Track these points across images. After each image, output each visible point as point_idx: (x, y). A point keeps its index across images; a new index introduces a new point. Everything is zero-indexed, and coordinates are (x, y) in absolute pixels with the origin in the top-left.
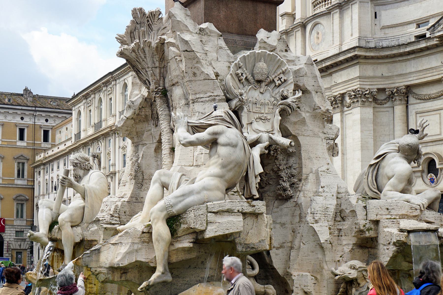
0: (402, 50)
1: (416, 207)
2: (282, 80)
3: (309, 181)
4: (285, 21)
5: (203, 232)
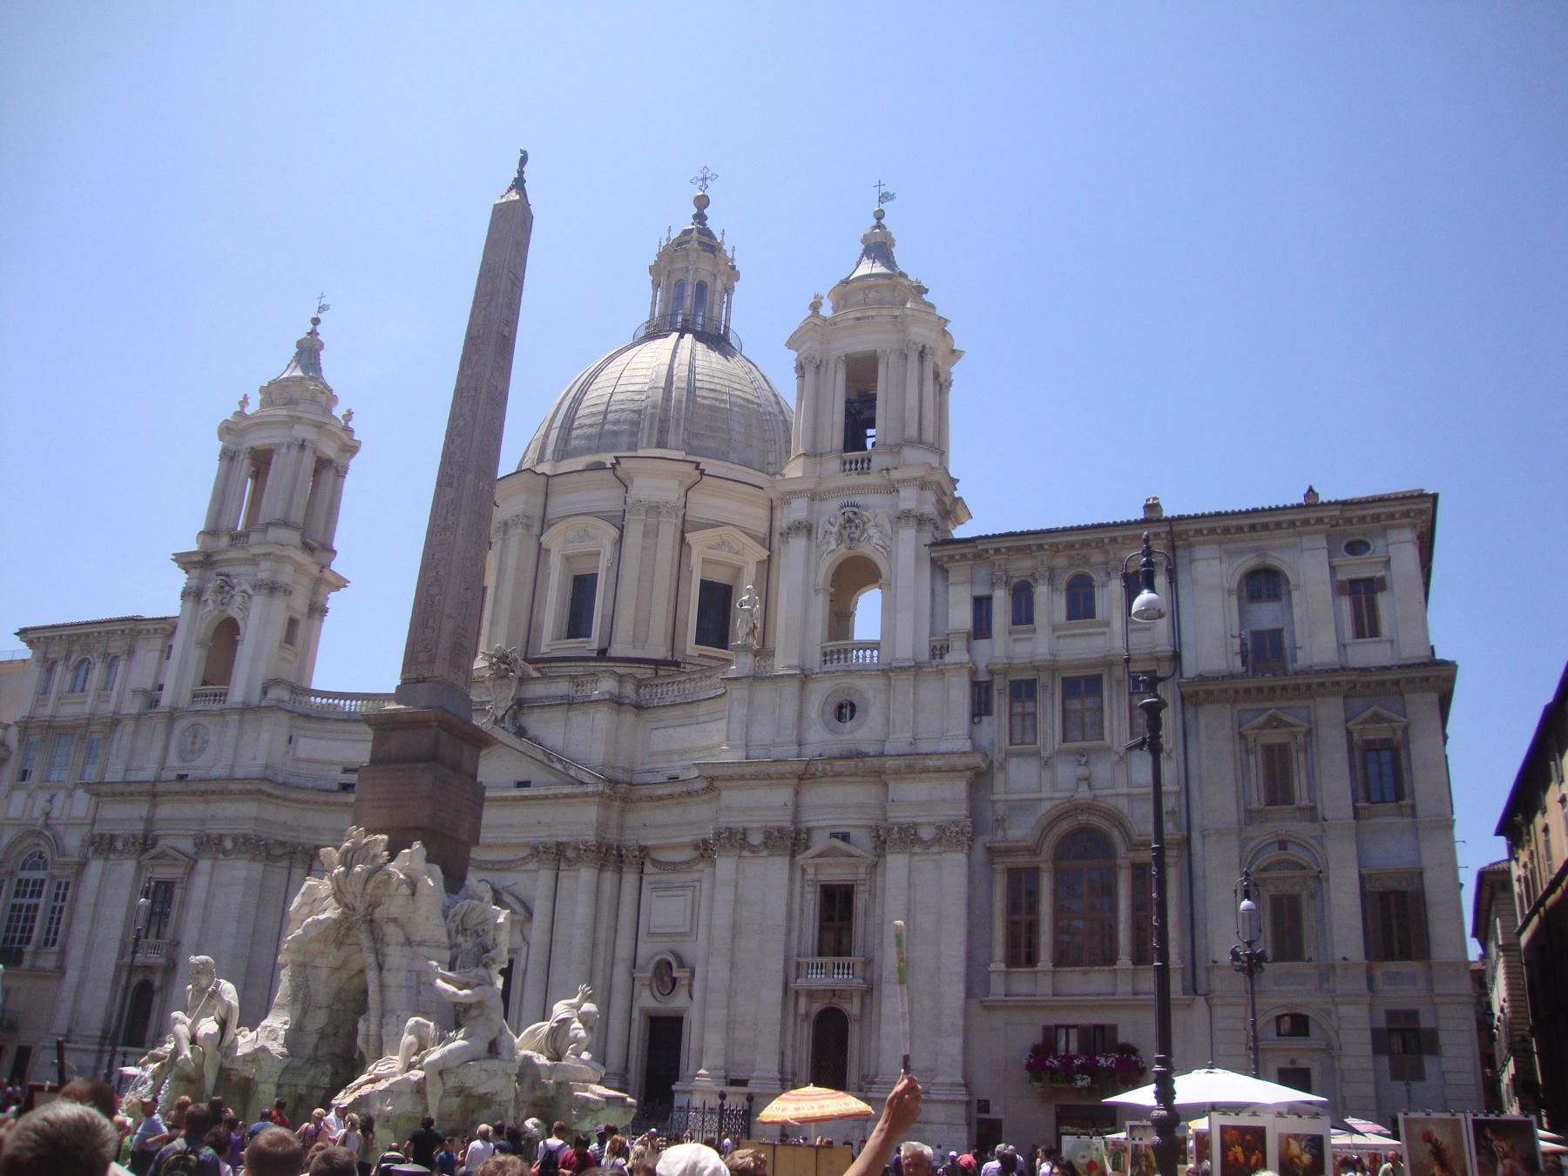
5: (470, 1088)
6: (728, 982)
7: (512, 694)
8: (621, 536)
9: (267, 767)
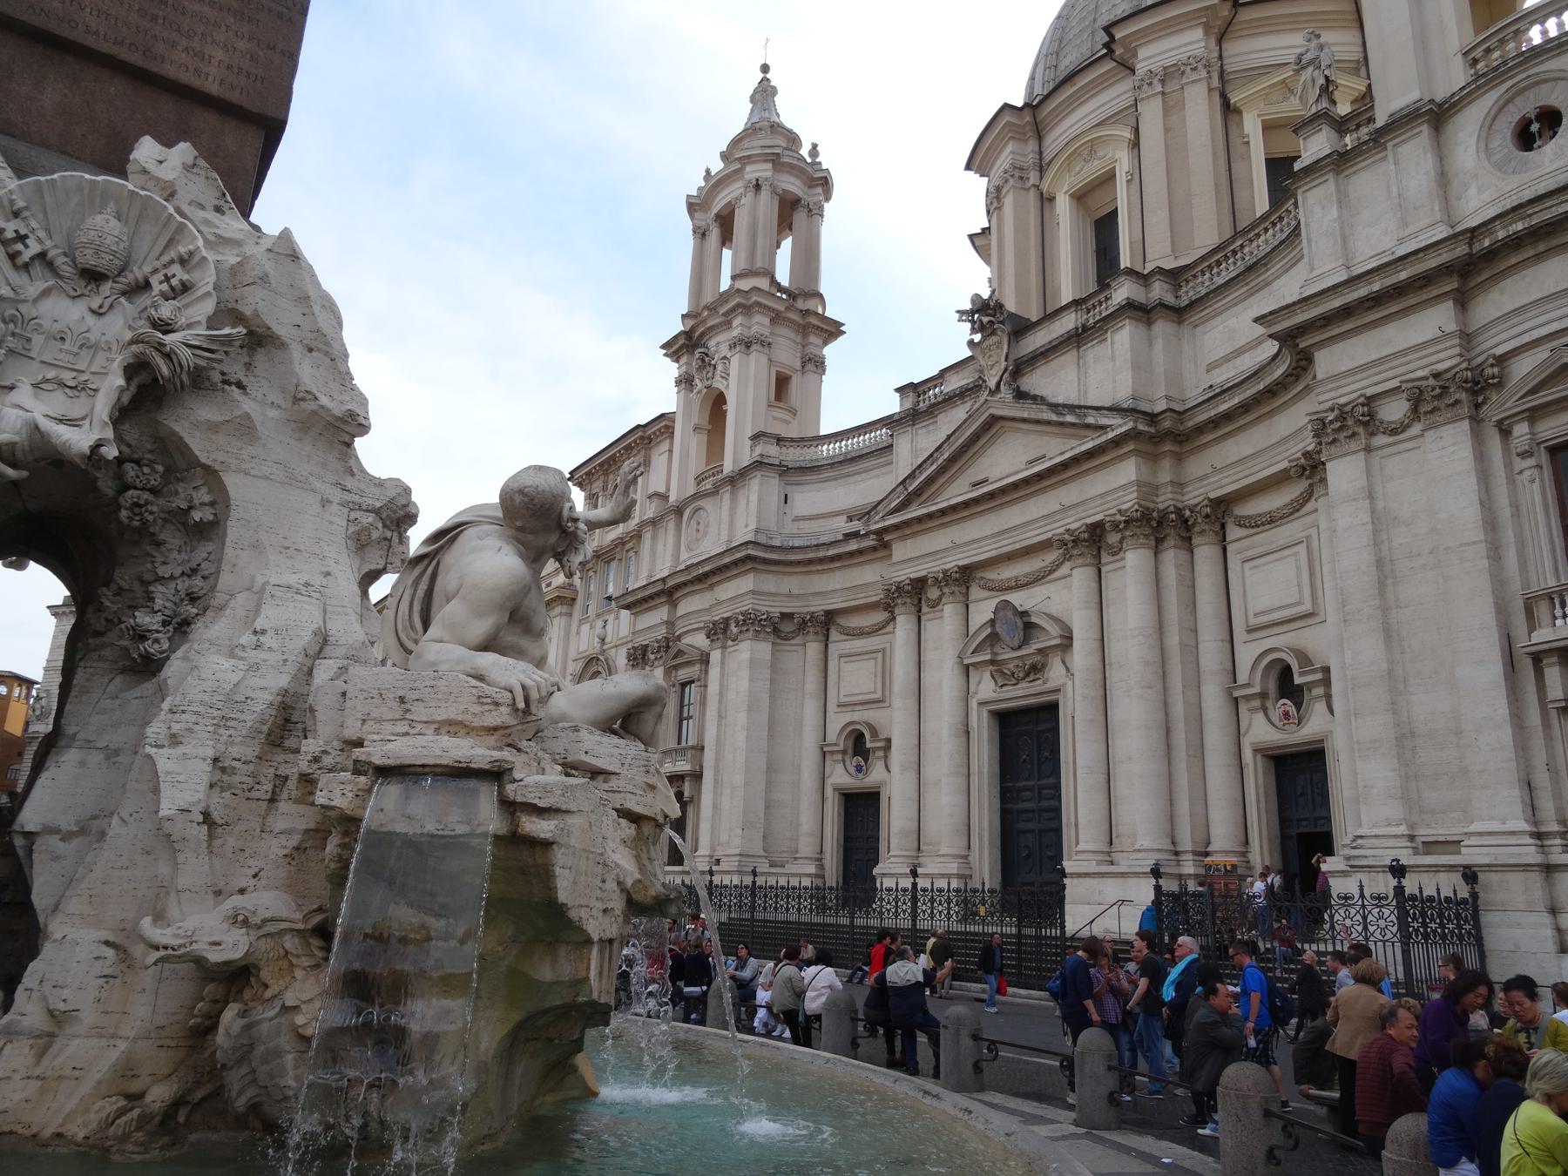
0: (821, 554)
1: (498, 696)
2: (174, 282)
3: (228, 612)
4: (653, 505)
6: (1385, 666)
7: (1005, 350)
8: (1137, 131)
9: (757, 531)
